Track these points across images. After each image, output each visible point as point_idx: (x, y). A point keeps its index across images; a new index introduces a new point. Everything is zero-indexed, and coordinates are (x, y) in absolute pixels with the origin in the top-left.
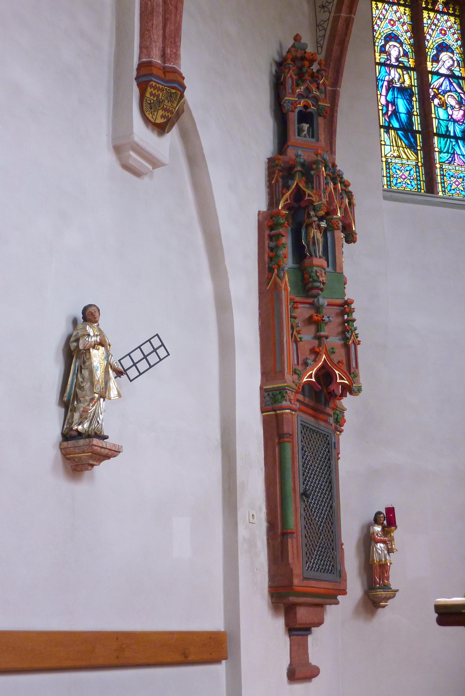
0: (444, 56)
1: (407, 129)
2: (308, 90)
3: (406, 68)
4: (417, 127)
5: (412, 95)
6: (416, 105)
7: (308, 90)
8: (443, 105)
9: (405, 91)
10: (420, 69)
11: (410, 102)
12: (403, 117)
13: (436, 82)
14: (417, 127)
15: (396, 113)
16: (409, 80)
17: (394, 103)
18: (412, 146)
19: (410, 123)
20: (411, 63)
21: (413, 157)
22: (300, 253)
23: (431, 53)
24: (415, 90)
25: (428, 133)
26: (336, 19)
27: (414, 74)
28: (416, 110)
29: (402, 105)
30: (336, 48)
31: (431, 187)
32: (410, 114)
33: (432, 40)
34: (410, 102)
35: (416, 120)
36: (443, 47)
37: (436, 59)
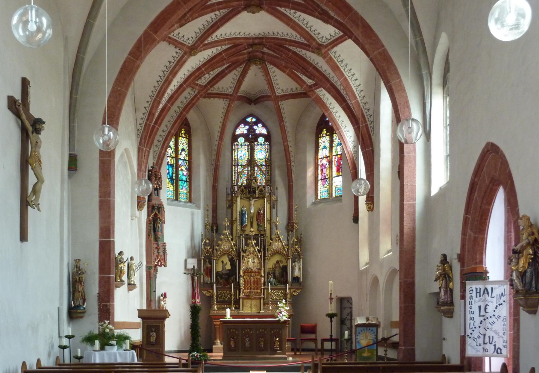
0: (183, 153)
1: (171, 178)
2: (157, 182)
3: (172, 157)
4: (174, 178)
5: (173, 167)
6: (174, 170)
7: (157, 182)
8: (181, 170)
9: (172, 165)
10: (177, 159)
11: (173, 169)
12: (171, 174)
13: (180, 162)
14: (174, 178)
15: (169, 173)
16: (172, 161)
17: (168, 170)
18: (172, 184)
19: (172, 176)
20: (174, 156)
21: (172, 187)
22: (155, 231)
23: (180, 152)
24: (174, 165)
25: (177, 179)
26: (161, 152)
27: (174, 159)
28: (174, 172)
29: (171, 170)
30: (160, 161)
31: (177, 199)
32: (172, 173)
33: (181, 147)
34: (173, 169)
35: (174, 175)
36: (183, 150)
37: (181, 154)
